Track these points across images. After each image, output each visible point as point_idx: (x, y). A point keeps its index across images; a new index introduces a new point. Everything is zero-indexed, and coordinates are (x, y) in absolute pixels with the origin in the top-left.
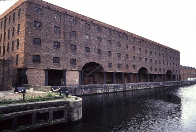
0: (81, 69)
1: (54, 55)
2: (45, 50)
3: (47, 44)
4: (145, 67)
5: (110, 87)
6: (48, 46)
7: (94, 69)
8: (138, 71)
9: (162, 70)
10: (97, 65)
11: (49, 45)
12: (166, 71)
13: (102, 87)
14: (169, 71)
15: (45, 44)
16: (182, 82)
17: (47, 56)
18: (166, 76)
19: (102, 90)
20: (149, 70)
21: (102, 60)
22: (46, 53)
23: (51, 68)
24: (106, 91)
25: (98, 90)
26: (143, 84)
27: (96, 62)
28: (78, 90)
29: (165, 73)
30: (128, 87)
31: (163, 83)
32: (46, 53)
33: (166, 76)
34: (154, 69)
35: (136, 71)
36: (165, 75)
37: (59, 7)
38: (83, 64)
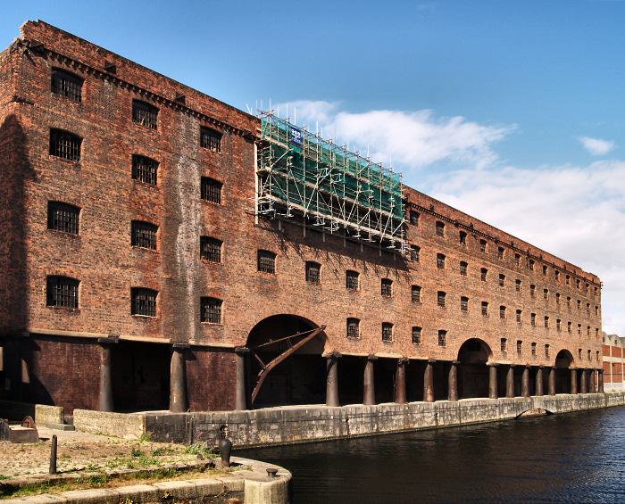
0: (244, 342)
1: (135, 279)
2: (97, 257)
3: (103, 232)
4: (482, 337)
5: (356, 416)
6: (107, 239)
7: (294, 341)
8: (456, 352)
9: (540, 350)
10: (304, 325)
11: (115, 234)
12: (554, 354)
13: (327, 418)
14: (564, 356)
15: (97, 228)
16: (607, 396)
17: (106, 282)
18: (552, 372)
19: (325, 428)
20: (495, 346)
21: (323, 307)
22: (102, 269)
23: (123, 337)
24: (341, 432)
25: (311, 428)
26: (473, 408)
27: (302, 313)
28: (234, 428)
29: (551, 363)
30: (422, 419)
31: (546, 402)
32: (102, 269)
33: (552, 372)
34: (511, 346)
35: (451, 353)
36: (546, 370)
37: (154, 73)
38: (252, 319)
